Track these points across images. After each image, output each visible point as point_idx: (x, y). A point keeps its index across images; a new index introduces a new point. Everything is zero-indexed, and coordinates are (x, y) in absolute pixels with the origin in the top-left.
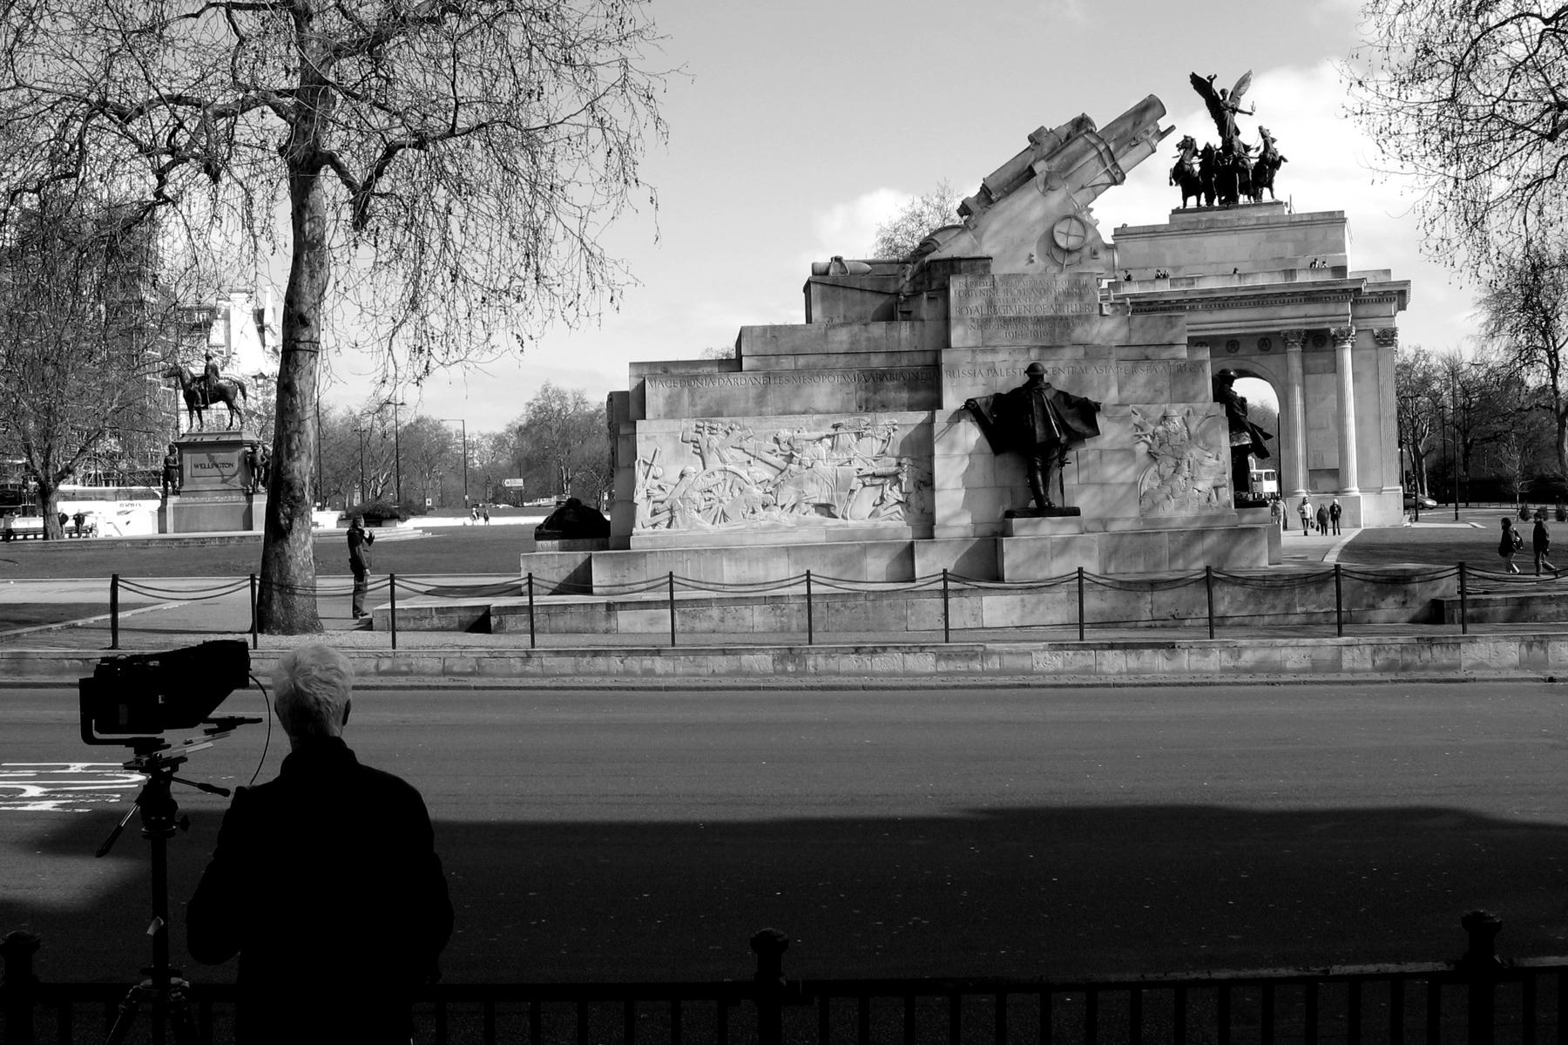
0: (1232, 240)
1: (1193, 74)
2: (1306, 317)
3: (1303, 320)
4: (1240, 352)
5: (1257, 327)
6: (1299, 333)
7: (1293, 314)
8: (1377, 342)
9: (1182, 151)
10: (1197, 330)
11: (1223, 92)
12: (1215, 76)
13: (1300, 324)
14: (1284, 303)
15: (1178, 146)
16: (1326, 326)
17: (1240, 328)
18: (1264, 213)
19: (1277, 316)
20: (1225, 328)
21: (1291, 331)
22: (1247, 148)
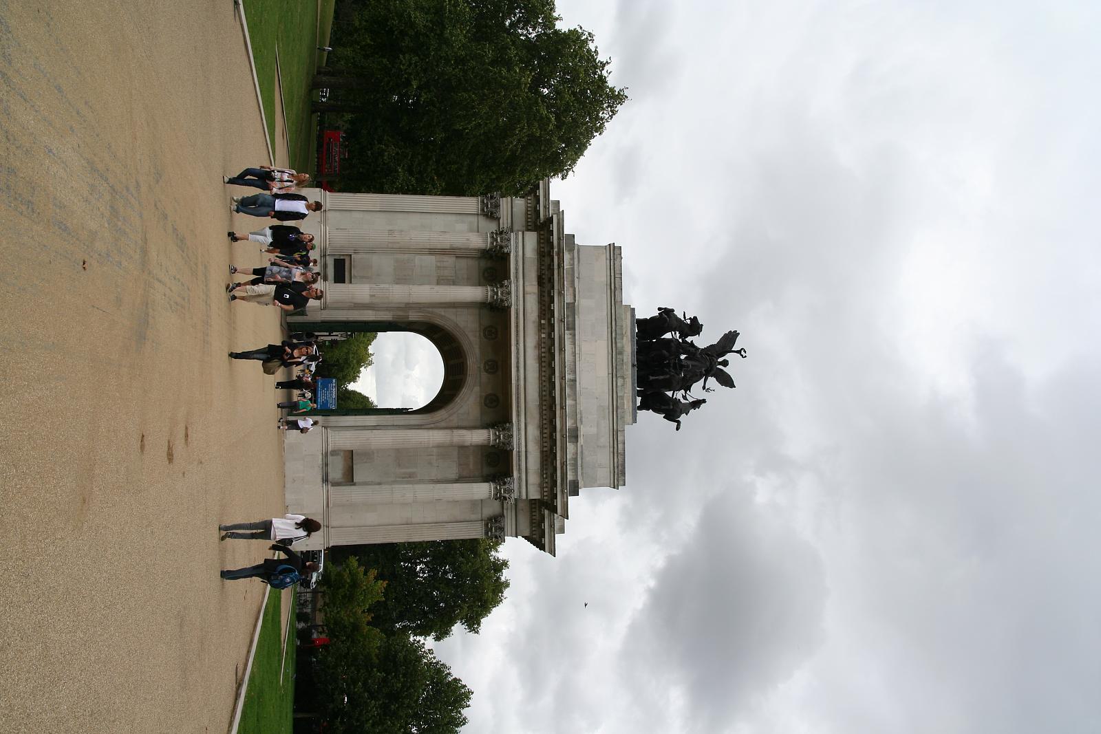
0: (603, 370)
2: (526, 451)
3: (523, 449)
4: (485, 375)
5: (518, 398)
6: (510, 443)
7: (530, 437)
8: (490, 519)
9: (689, 322)
10: (517, 331)
11: (725, 363)
13: (519, 445)
14: (542, 428)
15: (695, 318)
17: (518, 380)
18: (628, 406)
19: (528, 419)
20: (518, 362)
22: (688, 388)
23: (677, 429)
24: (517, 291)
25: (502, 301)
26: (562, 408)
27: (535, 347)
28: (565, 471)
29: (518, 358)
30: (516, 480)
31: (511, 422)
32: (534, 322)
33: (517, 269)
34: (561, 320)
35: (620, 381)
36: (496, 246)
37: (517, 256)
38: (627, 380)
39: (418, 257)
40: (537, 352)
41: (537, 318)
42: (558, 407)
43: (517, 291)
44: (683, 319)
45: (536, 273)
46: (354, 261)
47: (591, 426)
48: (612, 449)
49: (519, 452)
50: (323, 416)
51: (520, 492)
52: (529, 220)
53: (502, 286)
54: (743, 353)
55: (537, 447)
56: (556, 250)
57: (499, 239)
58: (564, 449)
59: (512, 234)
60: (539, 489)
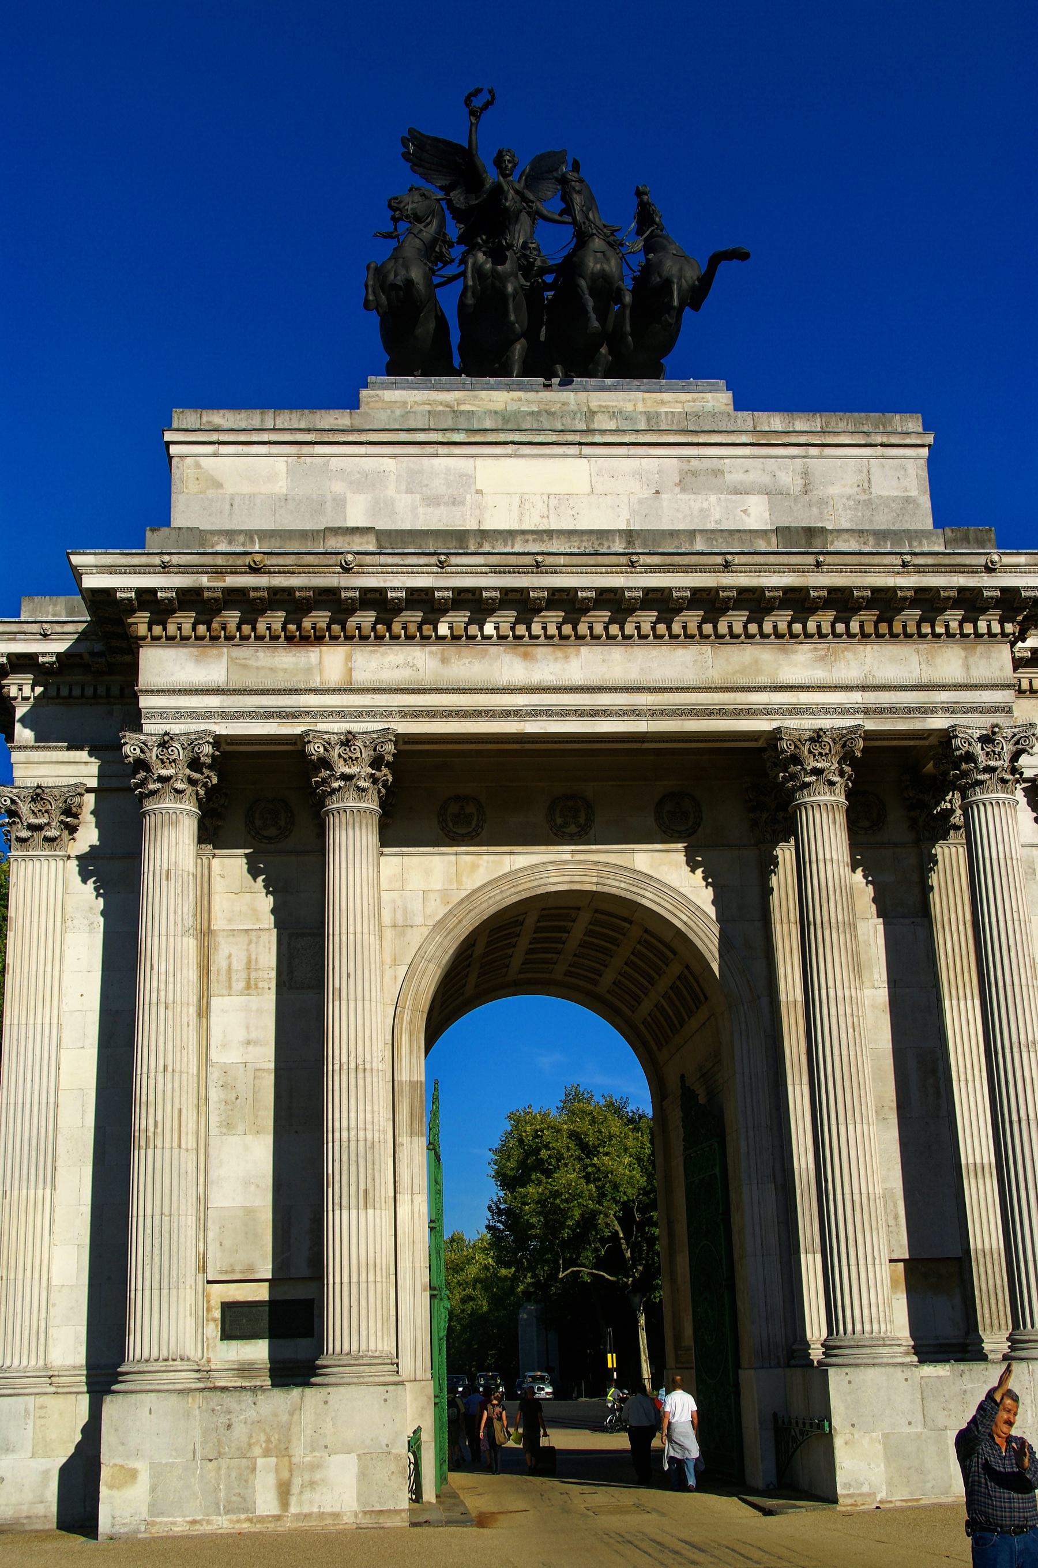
1: (414, 136)
2: (864, 688)
3: (857, 697)
5: (695, 712)
6: (844, 737)
7: (818, 675)
12: (491, 92)
16: (938, 723)
17: (635, 713)
19: (762, 680)
20: (579, 713)
21: (817, 737)
23: (744, 256)
24: (340, 714)
25: (377, 762)
26: (727, 565)
27: (526, 656)
28: (930, 560)
29: (565, 713)
30: (958, 722)
31: (775, 735)
32: (444, 661)
33: (269, 715)
34: (441, 565)
35: (603, 422)
36: (192, 782)
37: (224, 715)
38: (594, 405)
39: (215, 1056)
40: (540, 652)
41: (428, 649)
42: (727, 580)
43: (340, 714)
44: (394, 243)
45: (280, 650)
46: (233, 1271)
47: (745, 511)
48: (813, 451)
49: (867, 712)
50: (738, 1366)
51: (994, 710)
52: (89, 691)
53: (325, 763)
54: (478, 102)
55: (849, 655)
56: (204, 581)
57: (164, 772)
58: (859, 559)
59: (146, 728)
60: (980, 649)
